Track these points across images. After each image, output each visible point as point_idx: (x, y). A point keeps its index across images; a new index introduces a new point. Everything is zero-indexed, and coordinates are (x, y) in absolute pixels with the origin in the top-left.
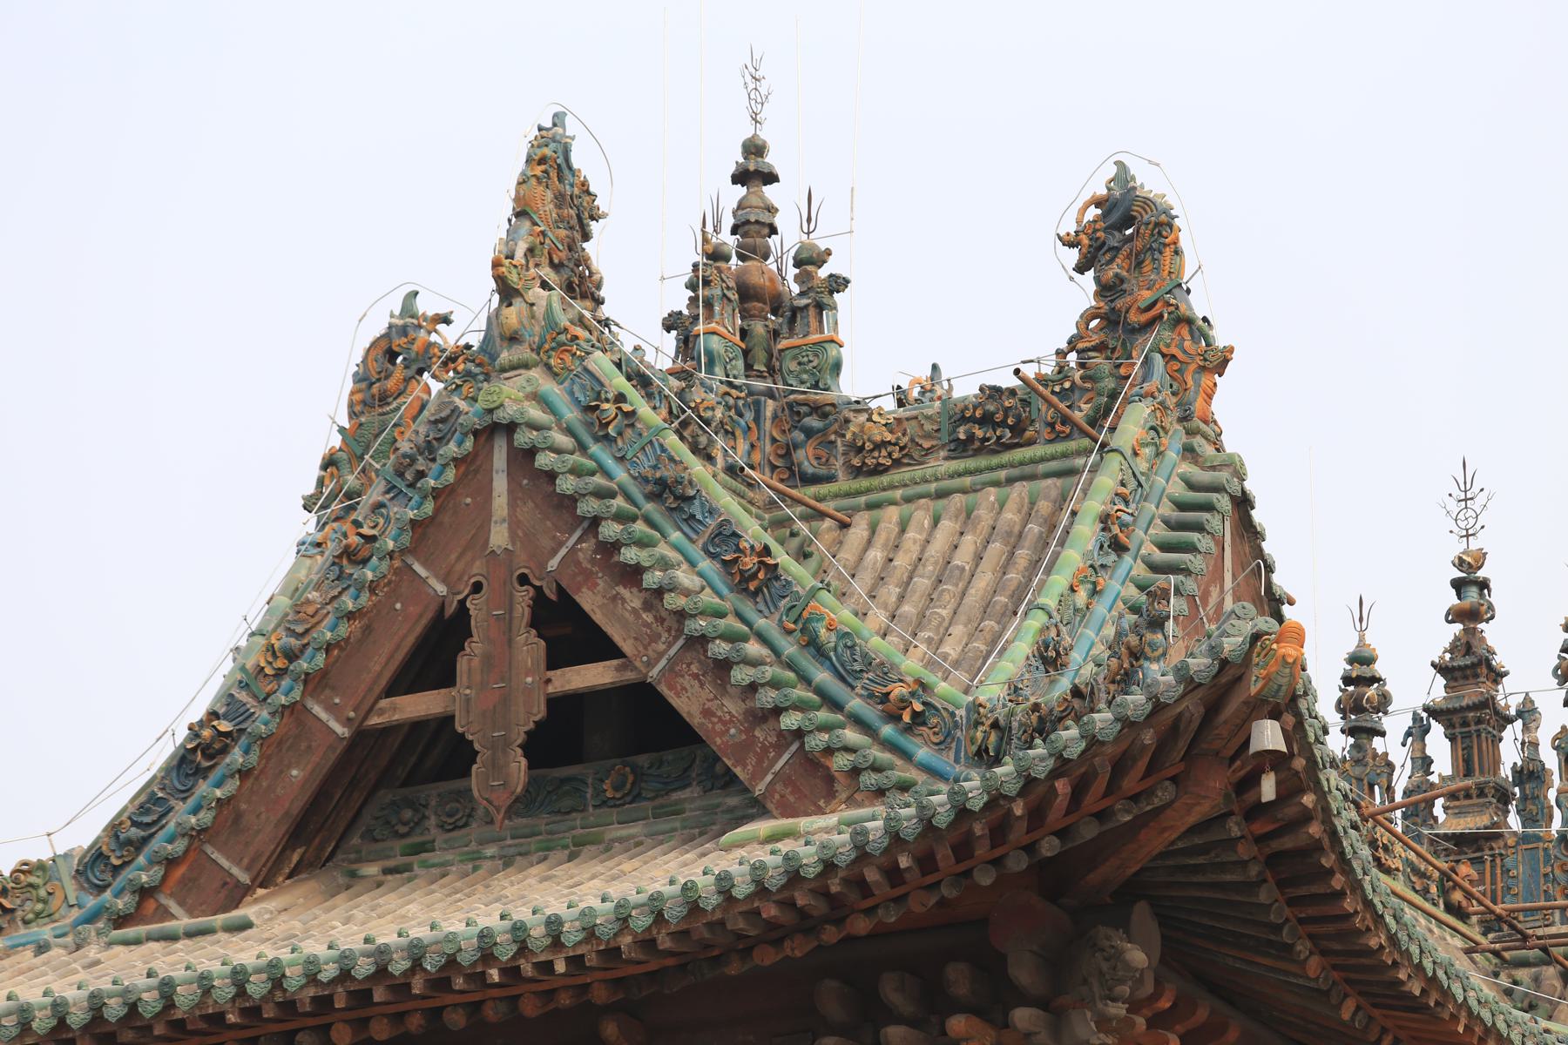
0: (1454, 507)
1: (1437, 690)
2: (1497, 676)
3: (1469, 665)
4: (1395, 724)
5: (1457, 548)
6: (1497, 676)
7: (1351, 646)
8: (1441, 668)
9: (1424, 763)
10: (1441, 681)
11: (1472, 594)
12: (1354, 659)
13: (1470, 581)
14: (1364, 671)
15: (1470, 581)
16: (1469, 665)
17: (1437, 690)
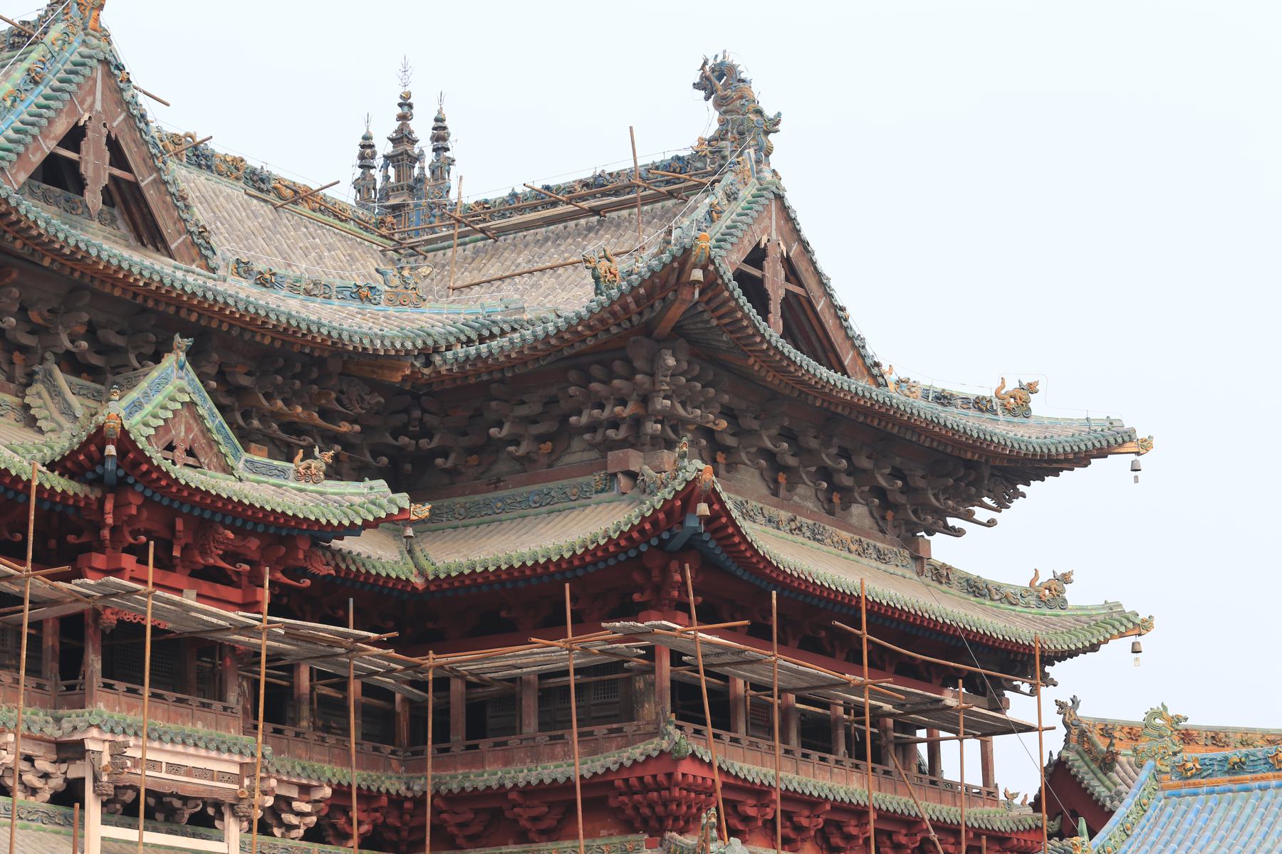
0: (401, 74)
1: (389, 148)
2: (415, 142)
3: (403, 137)
4: (379, 161)
5: (401, 90)
6: (415, 142)
7: (364, 133)
8: (391, 140)
9: (387, 178)
10: (391, 144)
11: (406, 109)
12: (365, 138)
13: (406, 103)
14: (367, 143)
15: (406, 103)
16: (403, 137)
17: (389, 148)
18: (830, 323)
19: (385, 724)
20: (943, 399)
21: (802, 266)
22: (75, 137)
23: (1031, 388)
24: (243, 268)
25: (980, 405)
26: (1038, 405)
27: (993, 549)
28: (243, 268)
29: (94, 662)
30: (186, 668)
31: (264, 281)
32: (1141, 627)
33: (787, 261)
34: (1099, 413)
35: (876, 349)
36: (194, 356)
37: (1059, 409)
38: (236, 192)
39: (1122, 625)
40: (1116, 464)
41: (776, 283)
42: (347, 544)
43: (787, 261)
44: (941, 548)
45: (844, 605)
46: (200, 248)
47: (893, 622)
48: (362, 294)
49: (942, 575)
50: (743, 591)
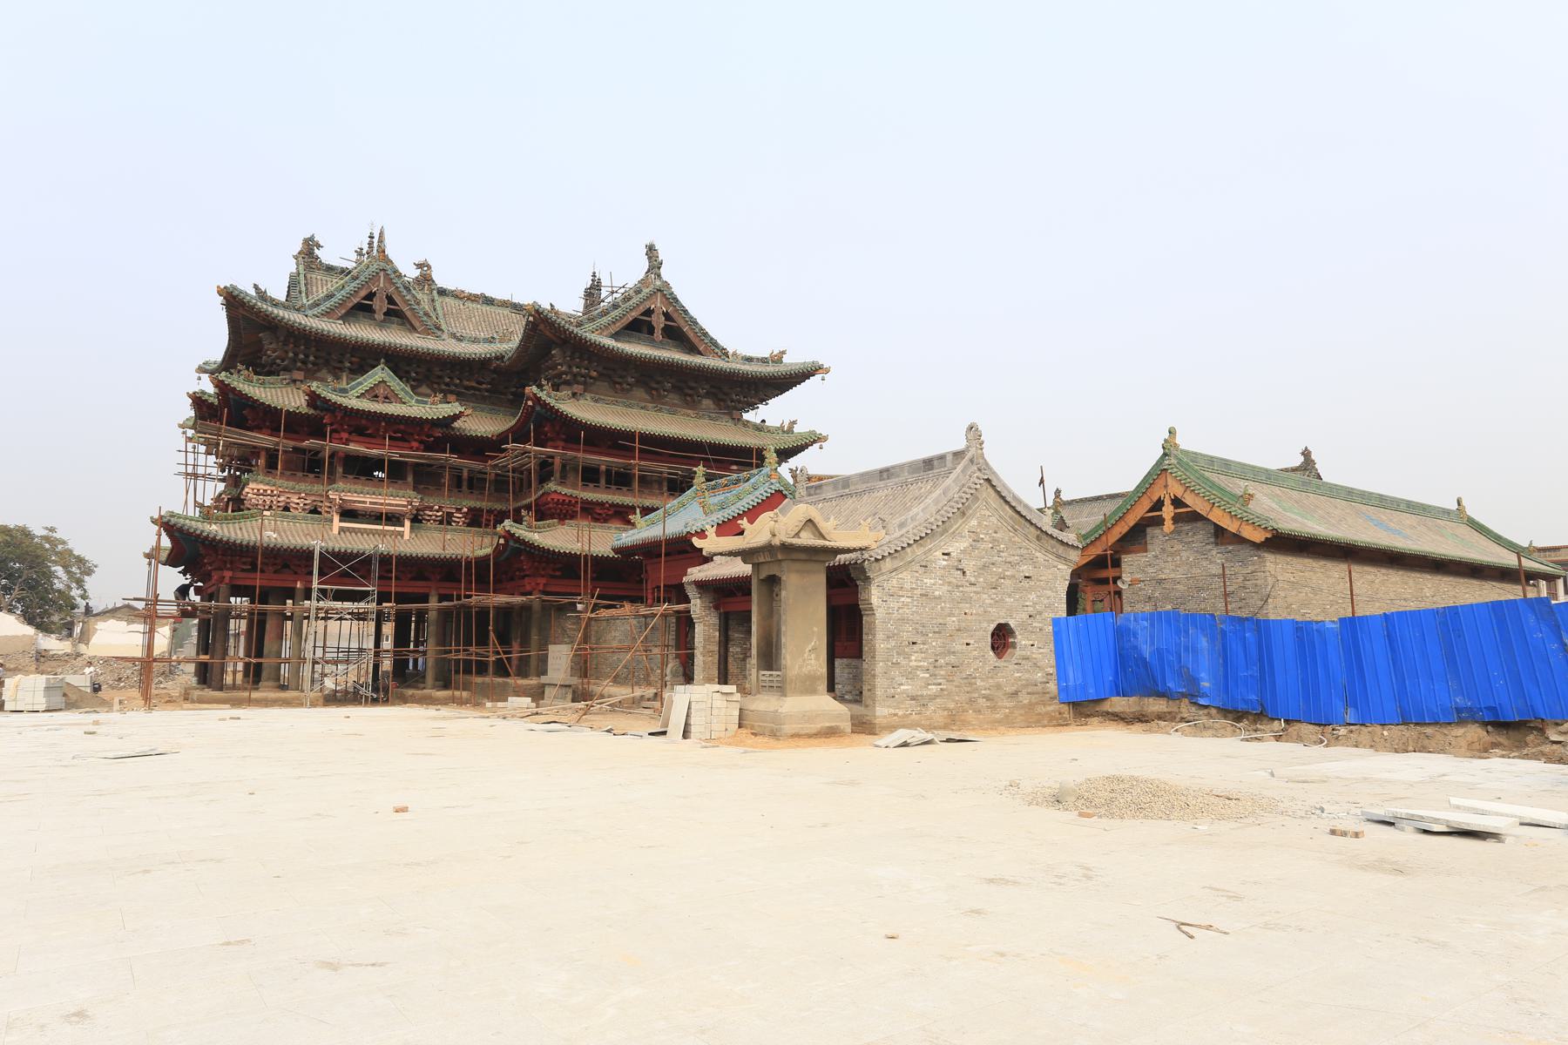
18: (691, 335)
19: (474, 483)
20: (749, 360)
21: (675, 316)
22: (371, 296)
23: (783, 352)
24: (454, 336)
25: (764, 361)
26: (786, 359)
27: (773, 412)
28: (454, 336)
29: (340, 470)
30: (361, 469)
31: (460, 339)
32: (825, 439)
33: (667, 316)
34: (810, 360)
35: (722, 342)
36: (386, 364)
37: (795, 359)
38: (506, 311)
39: (813, 439)
40: (818, 377)
41: (659, 322)
42: (456, 425)
43: (667, 316)
44: (746, 416)
45: (629, 435)
46: (435, 330)
47: (649, 440)
48: (491, 340)
49: (747, 424)
50: (572, 431)
